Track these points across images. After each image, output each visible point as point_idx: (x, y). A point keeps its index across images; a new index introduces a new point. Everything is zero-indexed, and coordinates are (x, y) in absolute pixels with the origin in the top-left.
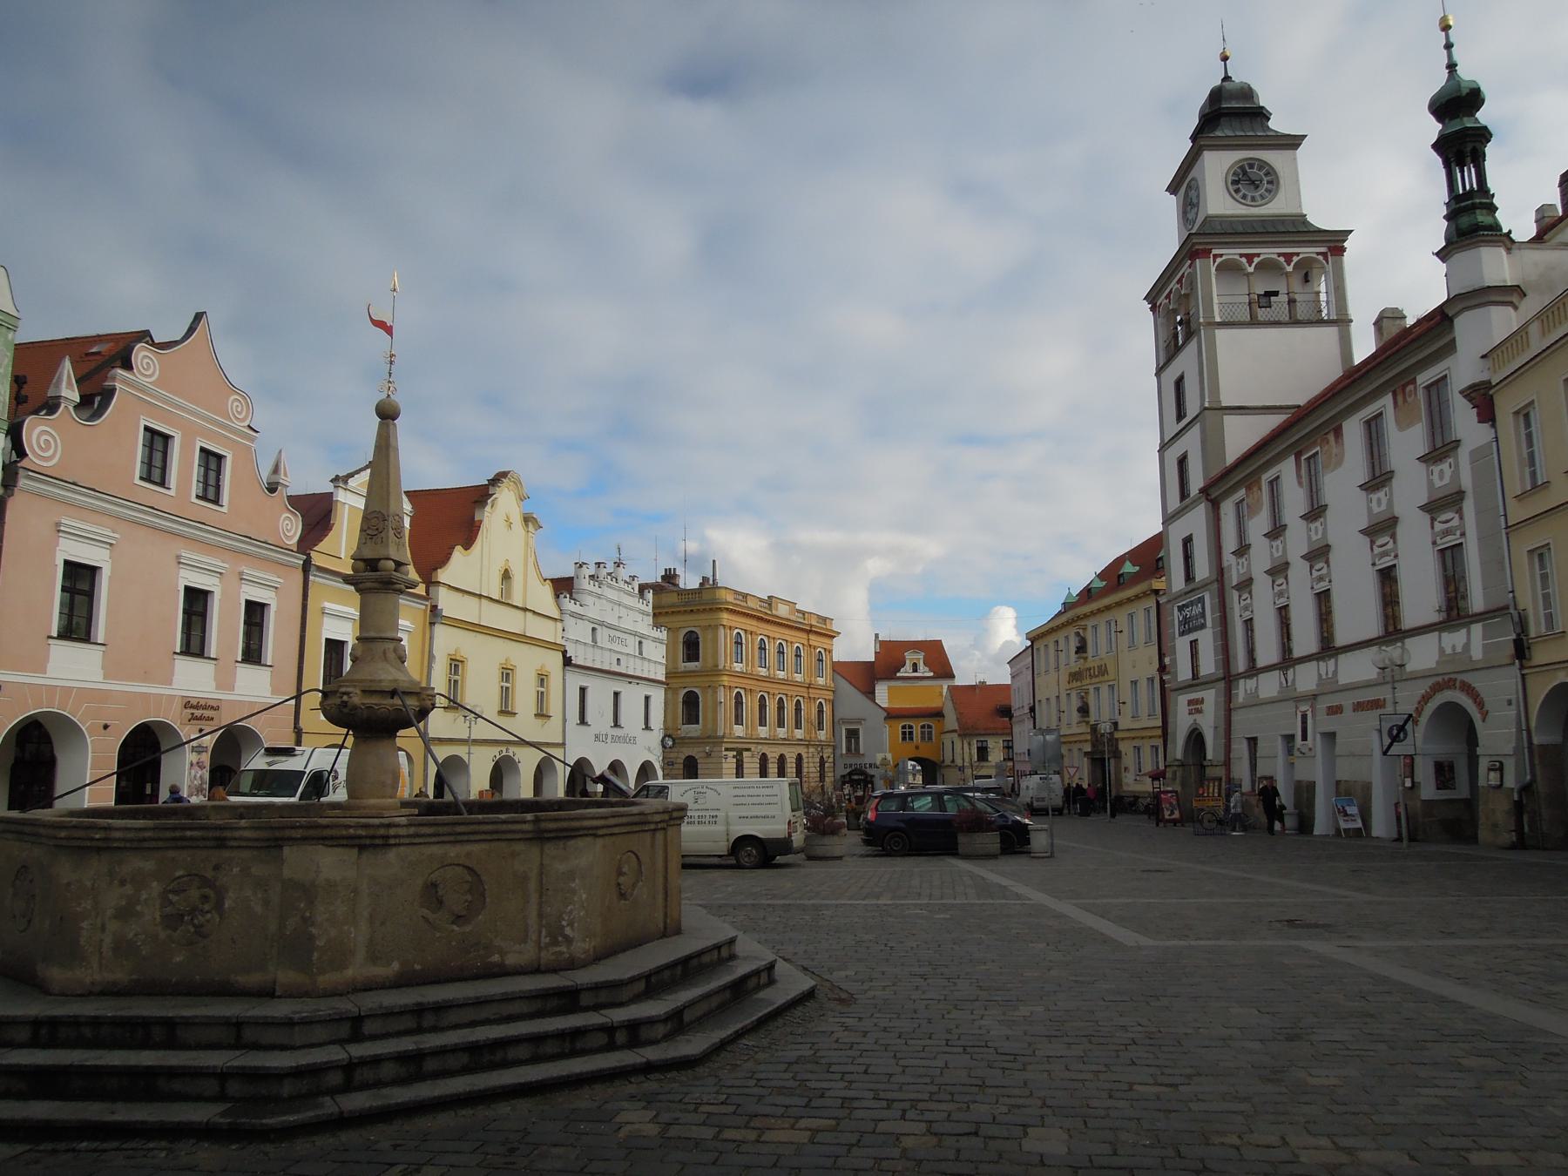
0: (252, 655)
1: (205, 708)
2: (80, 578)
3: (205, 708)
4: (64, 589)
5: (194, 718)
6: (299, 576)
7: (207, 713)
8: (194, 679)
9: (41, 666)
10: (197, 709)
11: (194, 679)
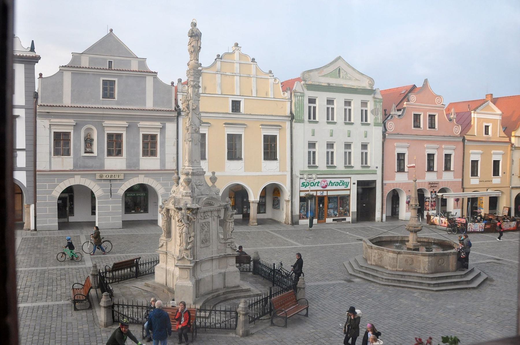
0: (447, 168)
1: (434, 184)
2: (401, 157)
3: (434, 184)
4: (398, 160)
5: (431, 187)
6: (461, 144)
7: (435, 185)
8: (431, 177)
9: (393, 179)
10: (432, 185)
11: (431, 177)
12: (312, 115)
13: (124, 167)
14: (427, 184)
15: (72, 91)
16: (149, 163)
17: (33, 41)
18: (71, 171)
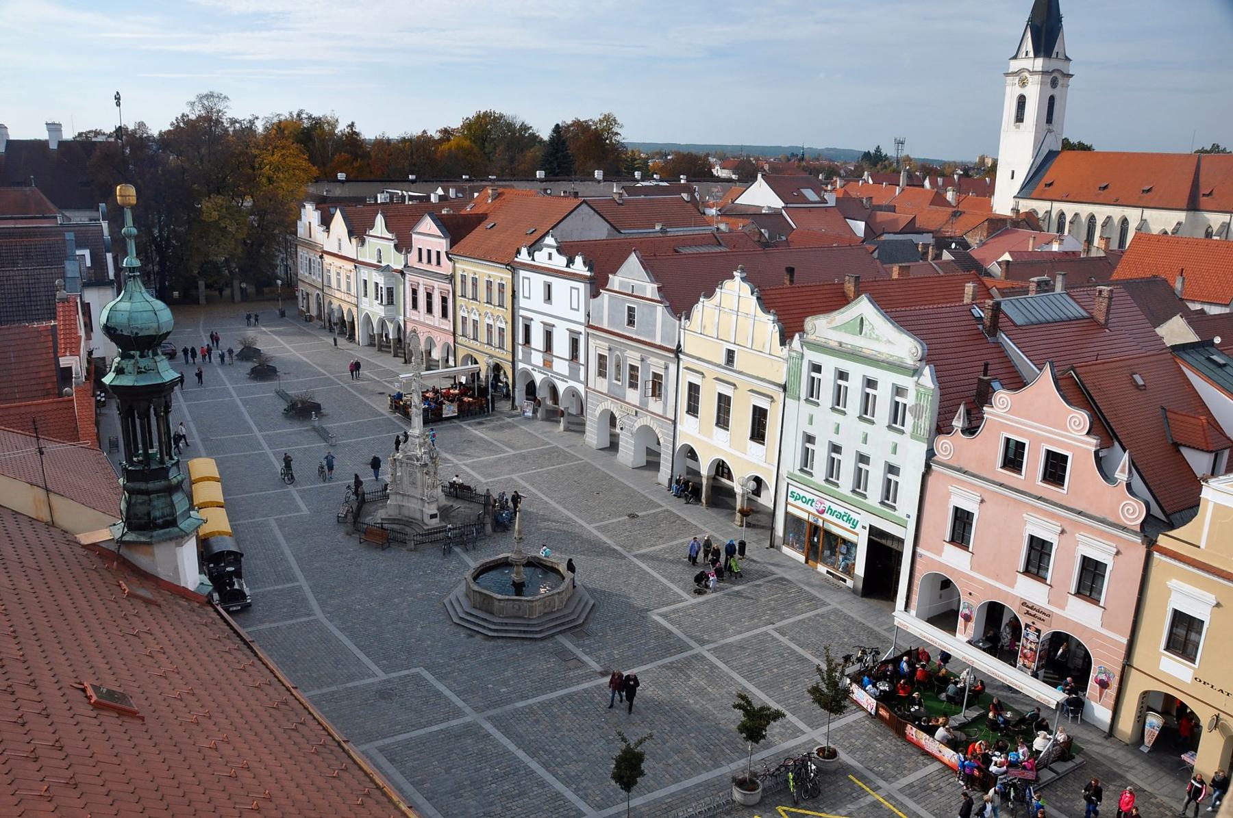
2: (962, 520)
6: (1142, 551)
9: (939, 553)
12: (814, 388)
14: (1018, 603)
16: (655, 406)
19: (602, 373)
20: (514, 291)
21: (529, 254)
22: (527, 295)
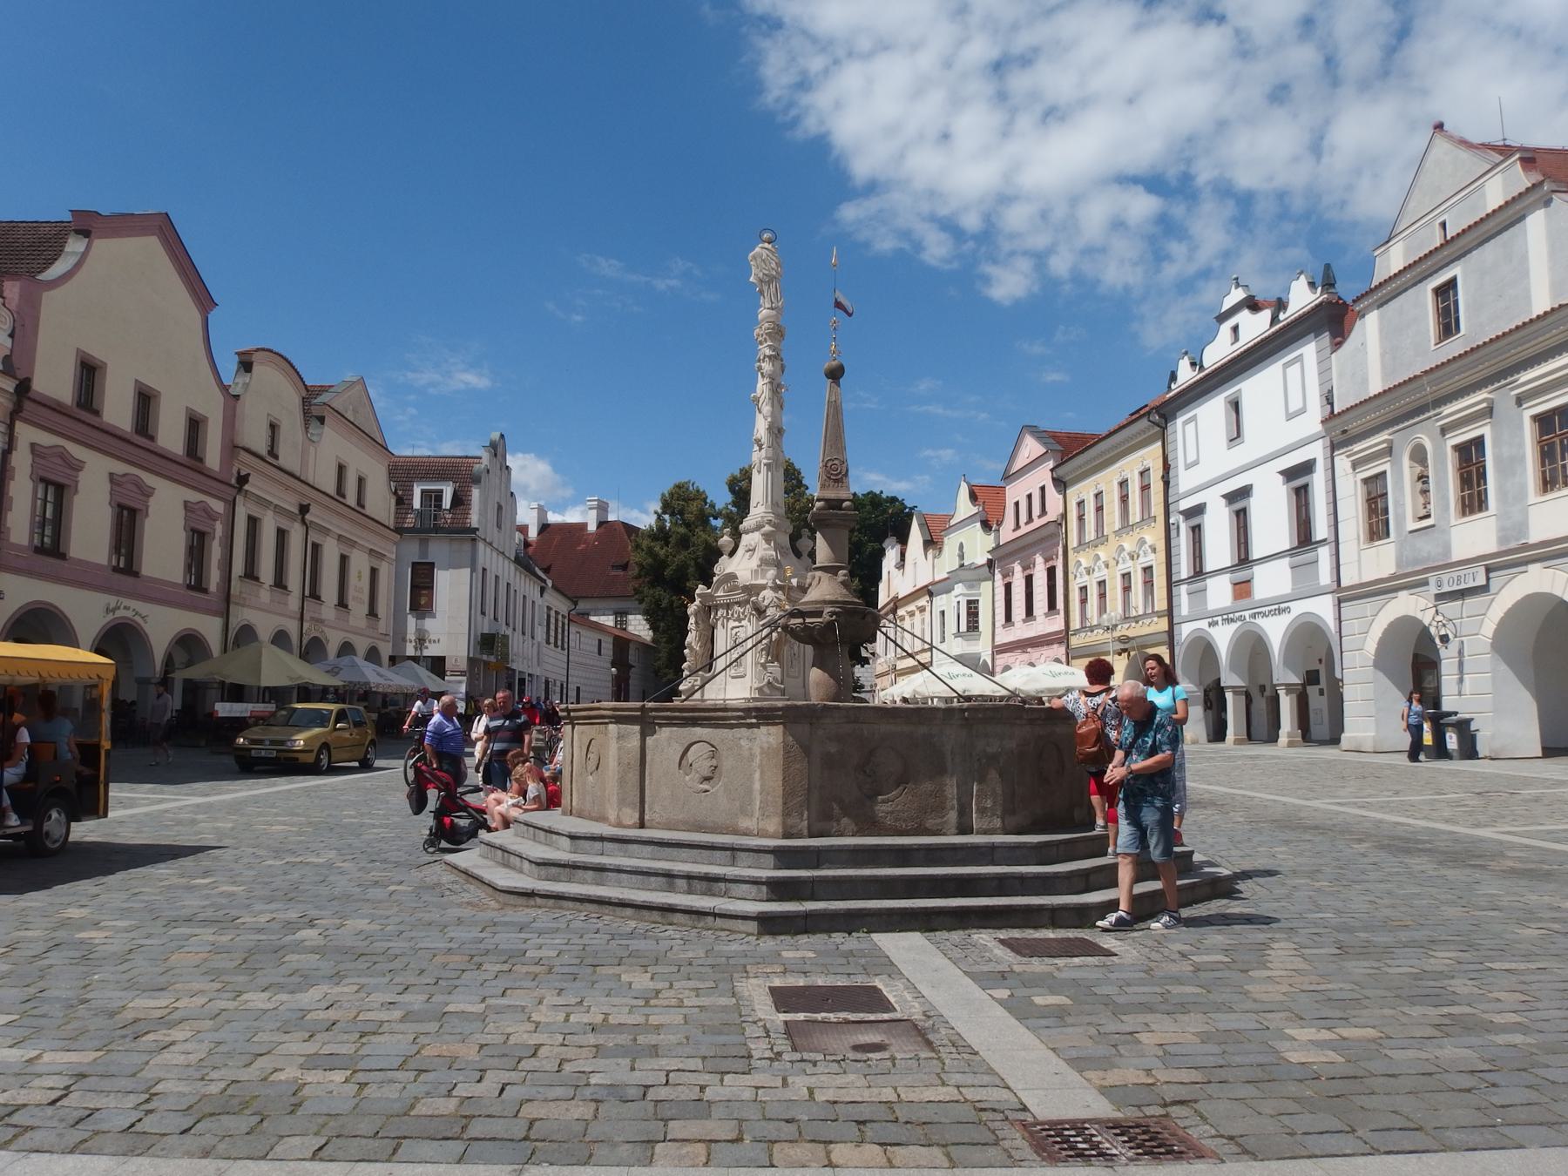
13: (1492, 547)
15: (1383, 355)
17: (1328, 267)
18: (1393, 577)
19: (1378, 528)
20: (1167, 467)
21: (1193, 364)
22: (1191, 458)
